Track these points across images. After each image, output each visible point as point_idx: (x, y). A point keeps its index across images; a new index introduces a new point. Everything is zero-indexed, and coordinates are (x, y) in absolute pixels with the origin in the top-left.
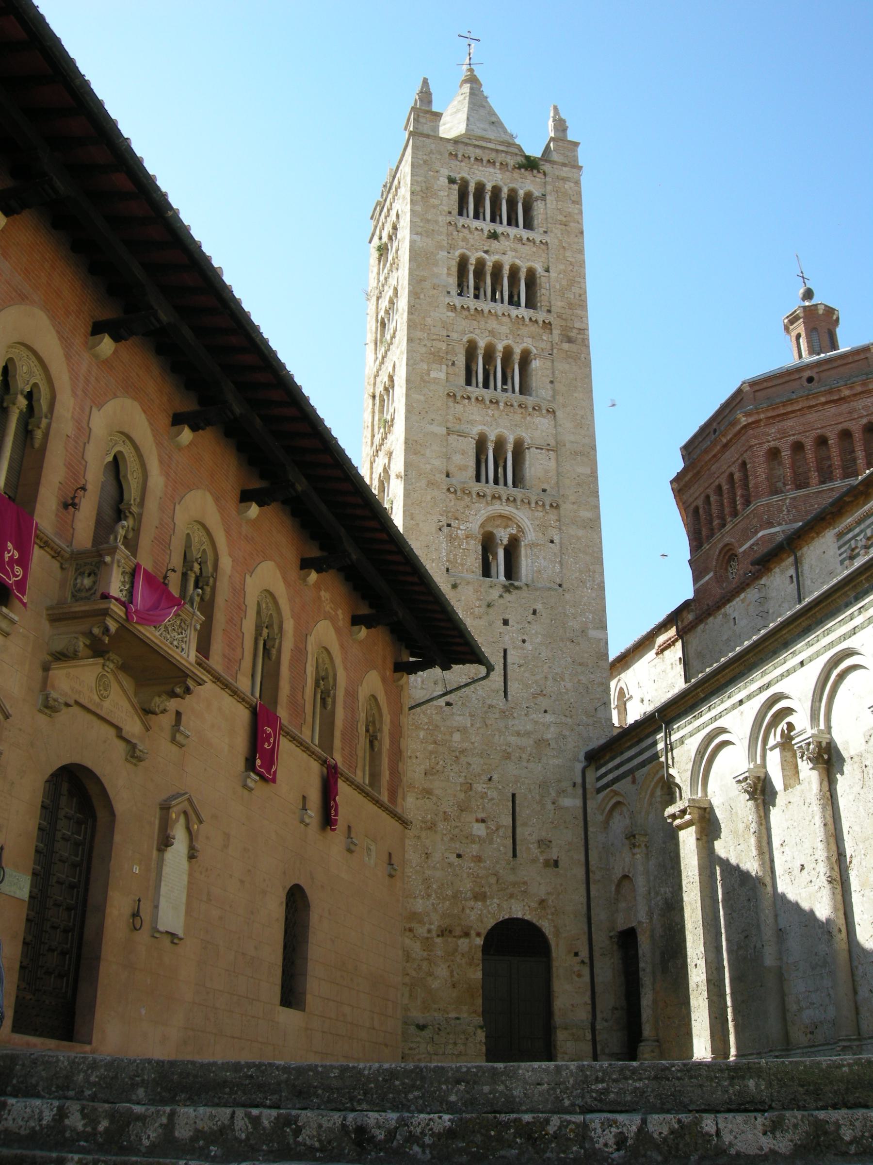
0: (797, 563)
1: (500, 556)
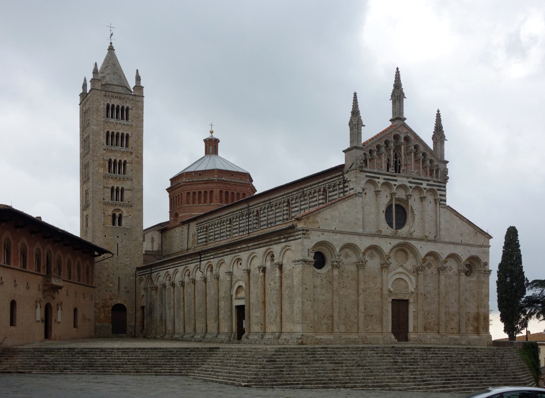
0: (189, 226)
1: (117, 219)
